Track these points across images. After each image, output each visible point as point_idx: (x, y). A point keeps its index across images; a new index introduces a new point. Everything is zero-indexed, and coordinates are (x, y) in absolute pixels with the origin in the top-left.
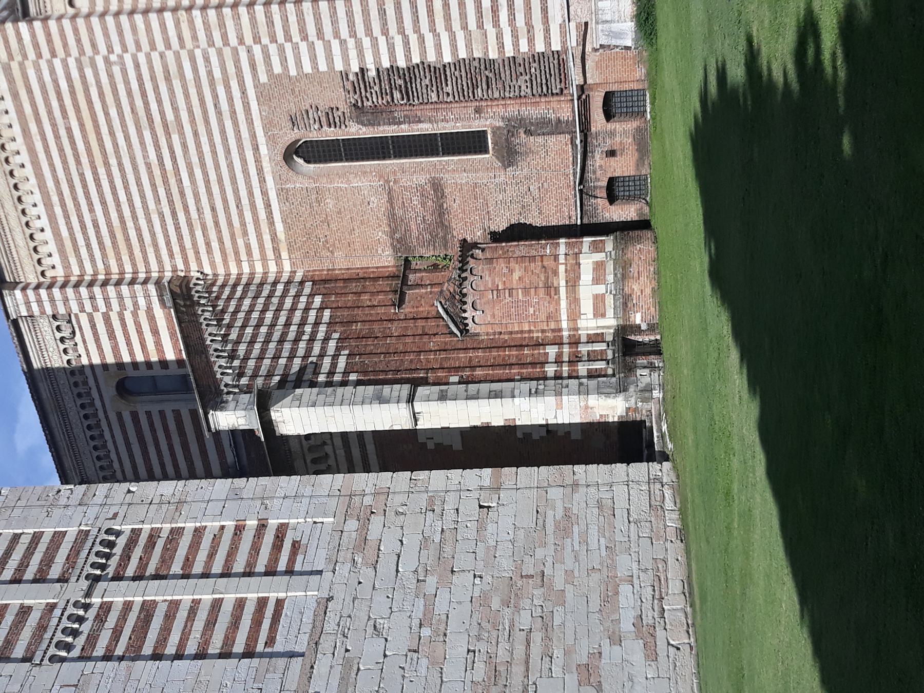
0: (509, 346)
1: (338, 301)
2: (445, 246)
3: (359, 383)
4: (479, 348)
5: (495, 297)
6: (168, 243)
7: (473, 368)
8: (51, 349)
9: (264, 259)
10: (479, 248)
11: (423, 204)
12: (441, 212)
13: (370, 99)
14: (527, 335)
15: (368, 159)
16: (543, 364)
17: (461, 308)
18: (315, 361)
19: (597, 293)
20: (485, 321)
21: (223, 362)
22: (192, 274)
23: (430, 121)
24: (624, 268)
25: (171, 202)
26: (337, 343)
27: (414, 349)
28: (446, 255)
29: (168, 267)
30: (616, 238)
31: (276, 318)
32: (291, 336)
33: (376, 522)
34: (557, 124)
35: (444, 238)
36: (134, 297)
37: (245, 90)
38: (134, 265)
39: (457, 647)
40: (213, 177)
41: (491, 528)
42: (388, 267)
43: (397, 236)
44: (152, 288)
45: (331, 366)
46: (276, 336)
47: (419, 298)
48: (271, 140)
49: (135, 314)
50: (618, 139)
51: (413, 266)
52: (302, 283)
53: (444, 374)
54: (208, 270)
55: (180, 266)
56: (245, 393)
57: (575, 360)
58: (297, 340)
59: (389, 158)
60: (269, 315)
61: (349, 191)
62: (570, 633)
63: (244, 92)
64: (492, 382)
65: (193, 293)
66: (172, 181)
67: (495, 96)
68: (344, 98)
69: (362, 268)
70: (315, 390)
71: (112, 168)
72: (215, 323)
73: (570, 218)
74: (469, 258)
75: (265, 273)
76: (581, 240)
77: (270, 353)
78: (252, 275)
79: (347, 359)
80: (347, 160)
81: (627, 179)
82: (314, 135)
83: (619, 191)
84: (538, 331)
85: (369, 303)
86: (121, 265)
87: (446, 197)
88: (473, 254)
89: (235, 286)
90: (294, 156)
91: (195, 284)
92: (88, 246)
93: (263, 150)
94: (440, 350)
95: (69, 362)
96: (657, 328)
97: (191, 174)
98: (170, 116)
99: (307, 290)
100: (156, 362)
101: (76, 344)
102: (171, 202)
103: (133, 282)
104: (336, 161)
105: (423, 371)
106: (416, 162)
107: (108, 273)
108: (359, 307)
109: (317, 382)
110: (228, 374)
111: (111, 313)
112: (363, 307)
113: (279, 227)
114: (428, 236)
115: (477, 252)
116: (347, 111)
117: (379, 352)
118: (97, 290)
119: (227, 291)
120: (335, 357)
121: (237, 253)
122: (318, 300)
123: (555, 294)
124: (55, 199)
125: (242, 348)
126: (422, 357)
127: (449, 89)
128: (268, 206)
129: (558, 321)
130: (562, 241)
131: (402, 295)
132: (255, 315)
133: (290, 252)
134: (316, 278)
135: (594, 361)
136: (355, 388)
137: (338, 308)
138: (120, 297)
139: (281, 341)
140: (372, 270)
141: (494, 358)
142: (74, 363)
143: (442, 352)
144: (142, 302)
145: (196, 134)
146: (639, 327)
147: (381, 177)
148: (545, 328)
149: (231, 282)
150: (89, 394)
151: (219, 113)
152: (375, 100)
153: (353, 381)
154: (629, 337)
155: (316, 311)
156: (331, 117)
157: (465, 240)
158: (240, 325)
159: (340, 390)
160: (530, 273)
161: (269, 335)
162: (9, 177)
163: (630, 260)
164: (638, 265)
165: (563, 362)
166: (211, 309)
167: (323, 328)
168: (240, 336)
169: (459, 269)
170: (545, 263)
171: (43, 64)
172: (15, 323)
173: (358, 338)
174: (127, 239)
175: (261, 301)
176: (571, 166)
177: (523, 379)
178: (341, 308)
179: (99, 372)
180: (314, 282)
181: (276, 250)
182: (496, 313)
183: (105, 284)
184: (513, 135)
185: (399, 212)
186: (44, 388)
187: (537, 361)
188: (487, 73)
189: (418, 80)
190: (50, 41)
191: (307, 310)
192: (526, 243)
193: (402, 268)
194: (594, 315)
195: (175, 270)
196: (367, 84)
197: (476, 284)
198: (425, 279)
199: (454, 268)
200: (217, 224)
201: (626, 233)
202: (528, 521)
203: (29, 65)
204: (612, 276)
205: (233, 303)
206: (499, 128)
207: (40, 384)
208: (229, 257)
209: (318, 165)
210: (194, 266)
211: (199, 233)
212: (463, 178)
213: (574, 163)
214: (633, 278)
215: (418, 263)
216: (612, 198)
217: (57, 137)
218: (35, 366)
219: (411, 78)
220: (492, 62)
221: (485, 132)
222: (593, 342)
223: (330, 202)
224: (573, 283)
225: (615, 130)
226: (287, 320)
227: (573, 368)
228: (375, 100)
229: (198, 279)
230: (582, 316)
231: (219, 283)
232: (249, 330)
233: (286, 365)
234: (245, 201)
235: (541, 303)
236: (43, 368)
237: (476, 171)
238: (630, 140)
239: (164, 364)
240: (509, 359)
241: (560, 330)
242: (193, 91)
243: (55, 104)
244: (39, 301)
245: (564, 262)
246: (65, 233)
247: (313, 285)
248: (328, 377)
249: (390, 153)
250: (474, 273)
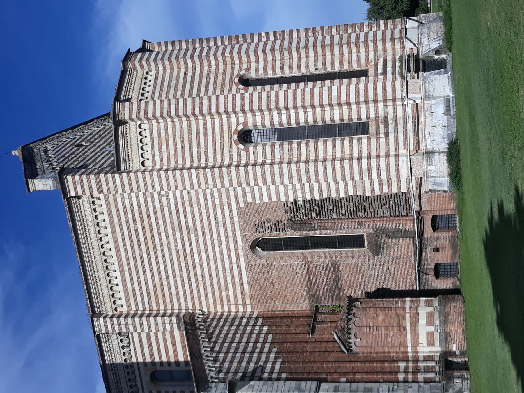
0: (376, 361)
1: (277, 330)
2: (339, 300)
3: (287, 379)
4: (358, 361)
5: (368, 331)
6: (185, 294)
7: (354, 373)
8: (116, 352)
9: (236, 304)
10: (359, 302)
11: (327, 275)
12: (337, 280)
13: (299, 216)
14: (386, 355)
15: (297, 249)
16: (397, 373)
17: (348, 336)
18: (262, 365)
19: (429, 331)
20: (362, 344)
21: (210, 364)
22: (196, 311)
23: (332, 229)
24: (445, 317)
25: (188, 271)
26: (275, 354)
27: (320, 360)
28: (340, 305)
29: (184, 307)
30: (440, 299)
31: (241, 338)
32: (249, 349)
34: (404, 232)
35: (339, 295)
36: (164, 324)
37: (232, 211)
38: (165, 306)
40: (211, 257)
42: (306, 310)
43: (312, 293)
44: (174, 319)
45: (271, 368)
46: (241, 349)
47: (323, 330)
49: (164, 334)
50: (440, 242)
51: (320, 311)
52: (257, 318)
53: (337, 376)
54: (205, 309)
55: (190, 307)
56: (222, 382)
57: (416, 371)
58: (252, 352)
59: (309, 249)
60: (238, 337)
61: (285, 267)
64: (366, 382)
66: (189, 259)
67: (369, 216)
68: (285, 216)
69: (291, 311)
70: (262, 383)
71: (158, 252)
72: (207, 340)
73: (412, 286)
74: (353, 307)
75: (237, 312)
76: (419, 299)
77: (237, 359)
78: (230, 312)
79: (281, 364)
80: (285, 250)
81: (446, 265)
82: (268, 235)
83: (442, 271)
84: (393, 353)
85: (294, 332)
86: (158, 305)
87: (340, 271)
88: (355, 305)
89: (220, 319)
90: (256, 247)
91: (198, 317)
92: (141, 294)
93: (240, 243)
94: (335, 362)
95: (125, 360)
96: (466, 353)
97: (200, 256)
99: (260, 323)
100: (173, 362)
101: (130, 350)
102: (188, 271)
103: (164, 315)
104: (279, 250)
105: (324, 374)
106: (324, 252)
107: (151, 310)
108: (288, 334)
109: (263, 378)
110: (213, 371)
111: (150, 332)
112: (291, 333)
113: (246, 286)
114: (329, 294)
115: (358, 304)
116: (286, 223)
117: (299, 361)
118: (144, 319)
119: (215, 322)
120: (274, 363)
121: (222, 300)
122: (265, 328)
123: (404, 331)
125: (222, 355)
126: (324, 365)
127: (343, 212)
128: (240, 274)
129: (406, 347)
130: (408, 299)
131: (314, 328)
132: (230, 336)
133: (251, 300)
134: (265, 316)
135: (428, 372)
136: (285, 382)
137: (277, 333)
138: (156, 324)
139: (244, 352)
140: (297, 312)
141: (367, 368)
142: (128, 361)
143: (336, 363)
144: (168, 327)
146: (455, 352)
147: (303, 259)
148: (398, 351)
149: (218, 317)
150: (135, 379)
152: (302, 217)
153: (283, 378)
154: (449, 359)
155: (264, 335)
156: (277, 226)
157: (351, 297)
158: (221, 342)
159: (276, 383)
160: (389, 317)
161: (237, 348)
162: (102, 255)
163: (449, 312)
164: (454, 316)
165: (409, 372)
166: (205, 332)
167: (267, 346)
168: (221, 348)
169: (347, 313)
170: (398, 312)
171: (126, 195)
172: (98, 337)
173: (288, 352)
174: (163, 291)
175: (234, 328)
176: (413, 256)
177: (385, 381)
178: (278, 334)
179: (141, 367)
180: (264, 318)
182: (368, 340)
183: (149, 316)
184: (379, 238)
185: (313, 279)
186: (110, 374)
187: (392, 371)
188: (365, 203)
189: (326, 207)
190: (130, 184)
191: (259, 334)
192: (387, 299)
193: (314, 311)
194: (428, 344)
195: (187, 309)
196: (298, 208)
197: (357, 322)
198: (327, 318)
199: (344, 313)
200: (212, 283)
201: (446, 296)
203: (118, 195)
204: (438, 321)
205: (218, 329)
206: (371, 234)
207: (109, 373)
208: (217, 302)
209: (269, 252)
210: (198, 307)
211: (202, 289)
212: (350, 261)
213: (415, 254)
214: (451, 323)
215: (323, 309)
216: (437, 275)
218: (107, 362)
219: (322, 205)
220: (367, 198)
221: (363, 236)
222: (427, 361)
223: (275, 273)
224: (415, 324)
225: (438, 237)
226: (247, 340)
227: (415, 376)
228: (302, 217)
229: (199, 314)
230: (420, 345)
231: (211, 317)
232: (226, 345)
233: (246, 366)
234: (228, 271)
235: (396, 336)
236: (111, 363)
237: (357, 257)
238: (447, 243)
239: (177, 363)
240: (376, 368)
241: (407, 352)
244: (112, 325)
245: (409, 311)
246: (129, 286)
247: (263, 319)
248: (269, 375)
249: (309, 246)
250: (356, 316)
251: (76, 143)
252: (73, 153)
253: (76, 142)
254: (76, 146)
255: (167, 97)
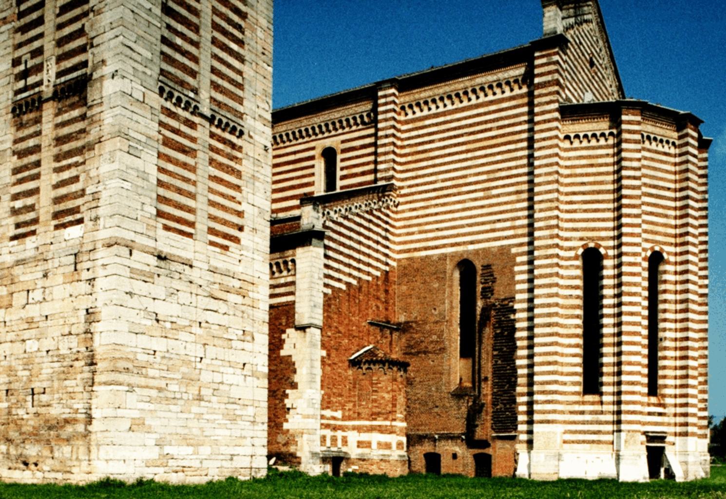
25: (442, 189)
33: (239, 299)
39: (160, 345)
41: (231, 370)
43: (414, 325)
48: (477, 252)
52: (387, 264)
62: (162, 414)
63: (507, 238)
65: (386, 198)
66: (455, 190)
93: (471, 247)
98: (494, 192)
102: (442, 189)
113: (423, 253)
121: (409, 226)
124: (448, 118)
128: (436, 247)
133: (408, 259)
145: (482, 207)
151: (494, 222)
180: (387, 272)
181: (408, 251)
200: (427, 215)
202: (235, 393)
217: (486, 122)
234: (440, 234)
242: (509, 207)
243: (506, 122)
246: (427, 122)
251: (594, 59)
252: (583, 55)
253: (596, 58)
254: (591, 59)
255: (644, 166)
